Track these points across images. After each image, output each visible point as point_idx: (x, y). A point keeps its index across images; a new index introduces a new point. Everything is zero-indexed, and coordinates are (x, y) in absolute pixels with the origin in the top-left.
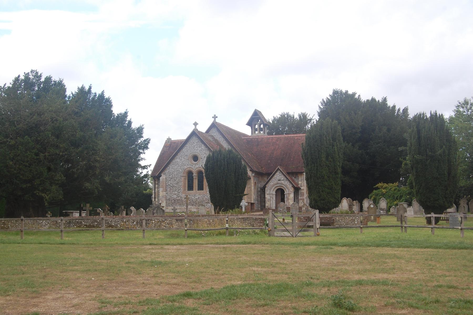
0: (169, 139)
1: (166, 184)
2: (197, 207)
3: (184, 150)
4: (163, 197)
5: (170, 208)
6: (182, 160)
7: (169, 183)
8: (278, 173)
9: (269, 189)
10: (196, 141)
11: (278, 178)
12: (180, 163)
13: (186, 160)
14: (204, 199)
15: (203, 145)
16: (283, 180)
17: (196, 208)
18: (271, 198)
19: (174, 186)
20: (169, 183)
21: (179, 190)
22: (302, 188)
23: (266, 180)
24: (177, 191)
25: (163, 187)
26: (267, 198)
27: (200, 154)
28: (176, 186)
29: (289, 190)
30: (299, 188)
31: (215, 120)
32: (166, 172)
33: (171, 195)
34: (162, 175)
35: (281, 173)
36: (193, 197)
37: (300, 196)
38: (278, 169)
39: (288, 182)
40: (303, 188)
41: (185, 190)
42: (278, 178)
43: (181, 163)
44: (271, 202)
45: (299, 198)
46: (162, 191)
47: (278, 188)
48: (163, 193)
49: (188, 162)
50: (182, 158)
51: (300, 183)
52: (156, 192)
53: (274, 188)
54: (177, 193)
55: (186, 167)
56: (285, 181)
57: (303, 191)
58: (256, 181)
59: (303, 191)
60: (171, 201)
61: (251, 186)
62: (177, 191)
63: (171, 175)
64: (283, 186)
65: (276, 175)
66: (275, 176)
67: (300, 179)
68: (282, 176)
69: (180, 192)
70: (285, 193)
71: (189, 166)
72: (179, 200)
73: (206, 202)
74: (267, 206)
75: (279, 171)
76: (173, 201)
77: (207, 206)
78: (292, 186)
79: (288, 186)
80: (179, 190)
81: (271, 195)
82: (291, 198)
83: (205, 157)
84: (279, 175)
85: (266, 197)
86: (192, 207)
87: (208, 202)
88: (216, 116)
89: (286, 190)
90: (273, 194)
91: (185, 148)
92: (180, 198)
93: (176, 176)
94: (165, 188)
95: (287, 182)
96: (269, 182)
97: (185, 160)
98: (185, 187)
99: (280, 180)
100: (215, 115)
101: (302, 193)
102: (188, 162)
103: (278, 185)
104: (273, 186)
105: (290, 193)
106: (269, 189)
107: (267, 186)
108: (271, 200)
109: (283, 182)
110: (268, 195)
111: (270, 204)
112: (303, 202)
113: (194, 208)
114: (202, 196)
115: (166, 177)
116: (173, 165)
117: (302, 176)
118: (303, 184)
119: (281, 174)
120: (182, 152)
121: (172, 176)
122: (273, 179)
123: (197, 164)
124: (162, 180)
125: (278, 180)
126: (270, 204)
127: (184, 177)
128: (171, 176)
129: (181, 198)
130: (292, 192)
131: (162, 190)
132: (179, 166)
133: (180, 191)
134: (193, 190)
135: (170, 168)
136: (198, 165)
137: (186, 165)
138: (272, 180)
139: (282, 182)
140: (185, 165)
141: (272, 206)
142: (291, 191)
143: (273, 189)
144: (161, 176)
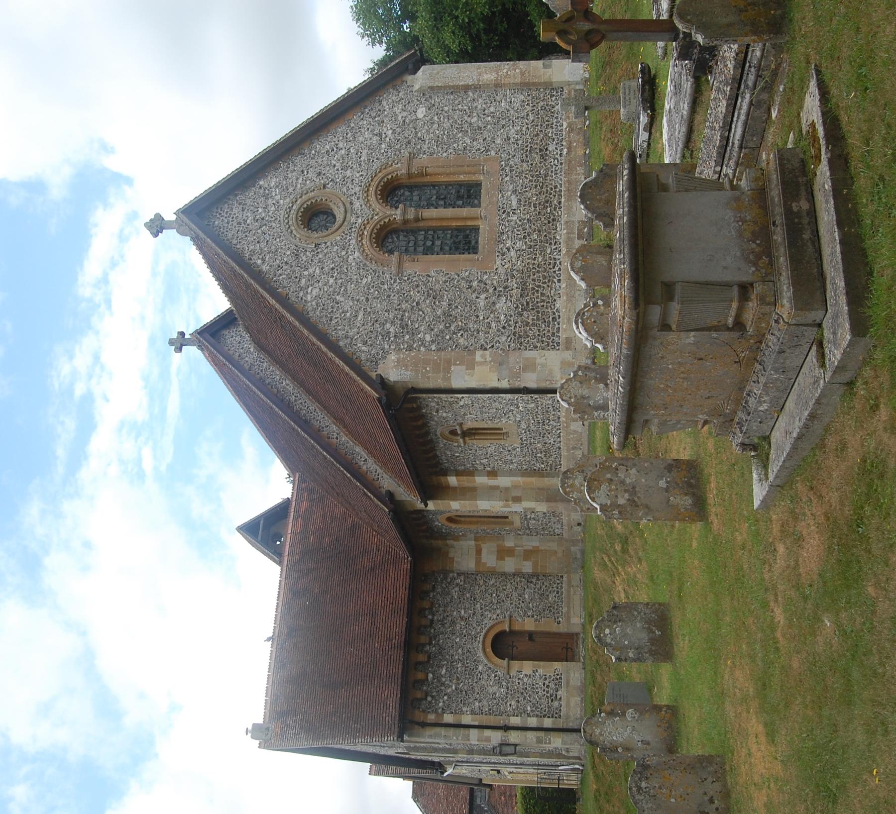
0: (257, 731)
3: (265, 268)
4: (500, 364)
5: (565, 330)
6: (318, 271)
7: (428, 338)
10: (235, 211)
13: (320, 256)
15: (261, 183)
17: (569, 199)
19: (446, 314)
20: (428, 338)
21: (470, 287)
24: (474, 296)
25: (449, 363)
32: (363, 357)
33: (493, 325)
36: (515, 218)
43: (332, 281)
48: (481, 364)
49: (329, 244)
50: (306, 273)
52: (476, 723)
54: (483, 296)
55: (357, 254)
60: (527, 324)
62: (474, 296)
63: (388, 325)
69: (480, 281)
71: (353, 242)
72: (524, 283)
76: (529, 316)
77: (558, 156)
80: (470, 287)
83: (319, 174)
86: (564, 218)
87: (541, 150)
88: (175, 336)
91: (259, 262)
92: (513, 284)
100: (171, 342)
102: (329, 244)
113: (569, 209)
114: (507, 179)
121: (393, 323)
123: (348, 205)
124: (406, 367)
127: (407, 264)
129: (513, 276)
131: (464, 367)
133: (475, 284)
135: (346, 337)
137: (343, 253)
140: (345, 260)
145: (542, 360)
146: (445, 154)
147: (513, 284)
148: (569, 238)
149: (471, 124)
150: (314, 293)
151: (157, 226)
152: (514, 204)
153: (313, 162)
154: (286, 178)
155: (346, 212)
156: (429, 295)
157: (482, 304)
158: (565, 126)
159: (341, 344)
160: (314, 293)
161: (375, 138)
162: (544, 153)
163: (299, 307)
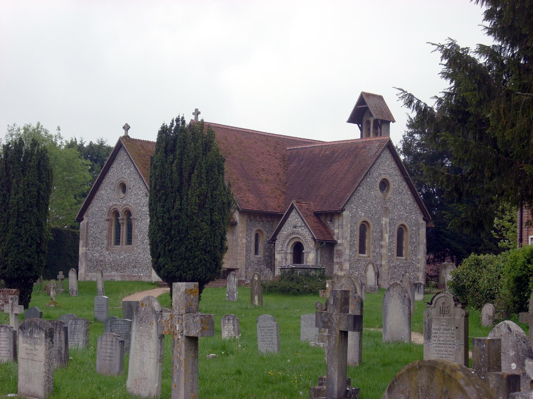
1: (87, 233)
2: (122, 274)
3: (110, 174)
6: (108, 192)
7: (92, 232)
8: (293, 213)
12: (105, 196)
14: (131, 260)
16: (300, 226)
18: (284, 260)
19: (96, 237)
22: (339, 241)
27: (128, 180)
28: (99, 236)
30: (335, 241)
31: (197, 118)
34: (84, 217)
37: (336, 258)
38: (292, 207)
39: (307, 230)
40: (341, 242)
41: (109, 244)
42: (293, 223)
45: (335, 260)
46: (83, 246)
47: (296, 240)
48: (83, 249)
50: (108, 188)
51: (336, 231)
53: (288, 240)
54: (100, 248)
56: (303, 228)
57: (340, 248)
58: (261, 229)
59: (340, 248)
61: (238, 237)
64: (301, 237)
65: (290, 216)
67: (336, 225)
68: (300, 219)
70: (303, 251)
73: (133, 265)
81: (283, 255)
82: (311, 261)
85: (276, 258)
91: (111, 171)
92: (102, 258)
93: (100, 220)
94: (85, 240)
96: (281, 231)
97: (111, 191)
98: (109, 238)
99: (295, 227)
100: (196, 110)
101: (339, 250)
103: (294, 236)
104: (287, 238)
106: (280, 242)
107: (277, 237)
109: (300, 230)
112: (339, 268)
114: (128, 254)
115: (88, 222)
116: (96, 201)
117: (340, 219)
118: (340, 235)
119: (297, 216)
120: (108, 178)
121: (96, 220)
122: (286, 225)
123: (124, 199)
128: (94, 220)
132: (104, 203)
133: (103, 246)
134: (119, 245)
135: (93, 206)
136: (126, 201)
138: (284, 226)
139: (298, 231)
144: (82, 219)
145: (83, 268)
146: (136, 231)
147: (102, 258)
148: (111, 276)
149: (145, 240)
150: (103, 192)
151: (127, 128)
152: (122, 257)
153: (137, 182)
154: (133, 173)
155: (123, 198)
156: (101, 231)
157: (98, 248)
158: (142, 274)
159: (92, 204)
160: (103, 192)
161: (143, 204)
162: (134, 267)
163: (100, 188)
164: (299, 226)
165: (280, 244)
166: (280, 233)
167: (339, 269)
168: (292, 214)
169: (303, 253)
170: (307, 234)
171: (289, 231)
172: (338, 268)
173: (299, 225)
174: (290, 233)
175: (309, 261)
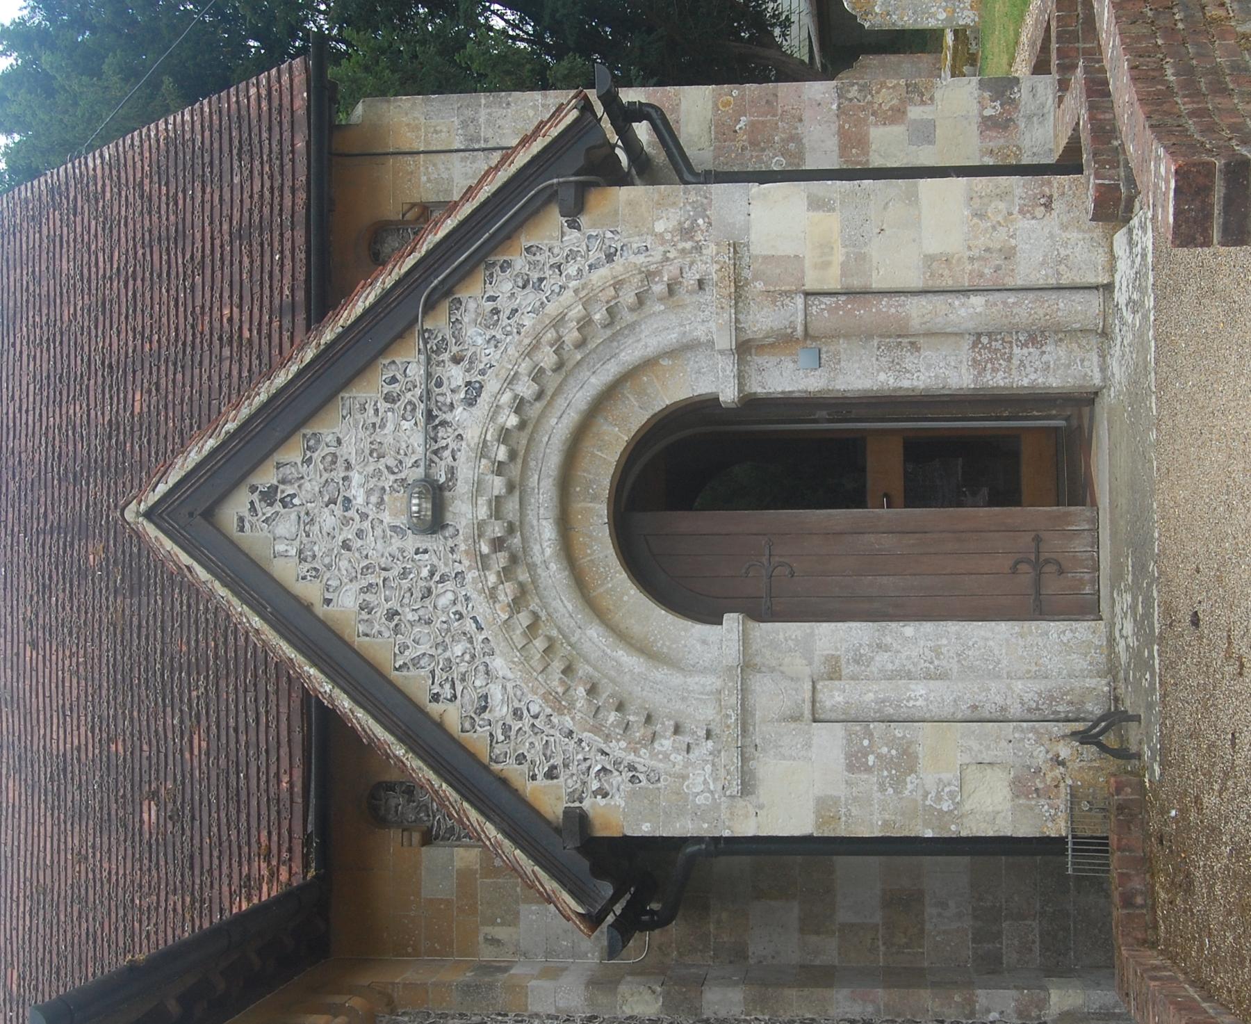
9: (618, 748)
11: (375, 548)
18: (835, 696)
23: (465, 857)
26: (824, 806)
29: (649, 276)
35: (267, 477)
39: (473, 297)
44: (919, 694)
53: (593, 637)
56: (456, 375)
65: (311, 591)
66: (347, 601)
74: (1022, 787)
75: (237, 507)
78: (574, 212)
79: (567, 303)
82: (831, 223)
84: (328, 519)
89: (648, 364)
90: (747, 666)
95: (474, 336)
96: (477, 740)
103: (545, 533)
105: (710, 262)
106: (618, 748)
108: (868, 695)
110: (768, 768)
111: (976, 718)
112: (897, 115)
125: (436, 523)
126: (976, 718)
130: (702, 210)
138: (417, 683)
139: (483, 450)
141: (1026, 691)
142: (686, 232)
143: (630, 661)
164: (431, 438)
165: (643, 759)
166: (509, 768)
167: (915, 112)
168: (287, 570)
169: (751, 404)
170: (528, 299)
171: (481, 608)
172: (898, 130)
173: (417, 440)
174: (507, 592)
175: (838, 256)
